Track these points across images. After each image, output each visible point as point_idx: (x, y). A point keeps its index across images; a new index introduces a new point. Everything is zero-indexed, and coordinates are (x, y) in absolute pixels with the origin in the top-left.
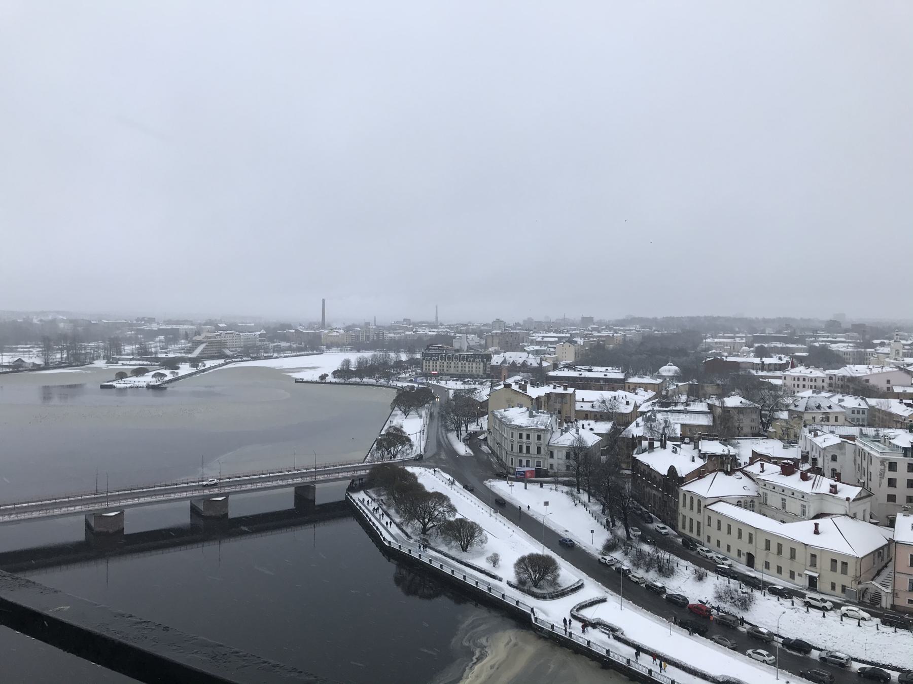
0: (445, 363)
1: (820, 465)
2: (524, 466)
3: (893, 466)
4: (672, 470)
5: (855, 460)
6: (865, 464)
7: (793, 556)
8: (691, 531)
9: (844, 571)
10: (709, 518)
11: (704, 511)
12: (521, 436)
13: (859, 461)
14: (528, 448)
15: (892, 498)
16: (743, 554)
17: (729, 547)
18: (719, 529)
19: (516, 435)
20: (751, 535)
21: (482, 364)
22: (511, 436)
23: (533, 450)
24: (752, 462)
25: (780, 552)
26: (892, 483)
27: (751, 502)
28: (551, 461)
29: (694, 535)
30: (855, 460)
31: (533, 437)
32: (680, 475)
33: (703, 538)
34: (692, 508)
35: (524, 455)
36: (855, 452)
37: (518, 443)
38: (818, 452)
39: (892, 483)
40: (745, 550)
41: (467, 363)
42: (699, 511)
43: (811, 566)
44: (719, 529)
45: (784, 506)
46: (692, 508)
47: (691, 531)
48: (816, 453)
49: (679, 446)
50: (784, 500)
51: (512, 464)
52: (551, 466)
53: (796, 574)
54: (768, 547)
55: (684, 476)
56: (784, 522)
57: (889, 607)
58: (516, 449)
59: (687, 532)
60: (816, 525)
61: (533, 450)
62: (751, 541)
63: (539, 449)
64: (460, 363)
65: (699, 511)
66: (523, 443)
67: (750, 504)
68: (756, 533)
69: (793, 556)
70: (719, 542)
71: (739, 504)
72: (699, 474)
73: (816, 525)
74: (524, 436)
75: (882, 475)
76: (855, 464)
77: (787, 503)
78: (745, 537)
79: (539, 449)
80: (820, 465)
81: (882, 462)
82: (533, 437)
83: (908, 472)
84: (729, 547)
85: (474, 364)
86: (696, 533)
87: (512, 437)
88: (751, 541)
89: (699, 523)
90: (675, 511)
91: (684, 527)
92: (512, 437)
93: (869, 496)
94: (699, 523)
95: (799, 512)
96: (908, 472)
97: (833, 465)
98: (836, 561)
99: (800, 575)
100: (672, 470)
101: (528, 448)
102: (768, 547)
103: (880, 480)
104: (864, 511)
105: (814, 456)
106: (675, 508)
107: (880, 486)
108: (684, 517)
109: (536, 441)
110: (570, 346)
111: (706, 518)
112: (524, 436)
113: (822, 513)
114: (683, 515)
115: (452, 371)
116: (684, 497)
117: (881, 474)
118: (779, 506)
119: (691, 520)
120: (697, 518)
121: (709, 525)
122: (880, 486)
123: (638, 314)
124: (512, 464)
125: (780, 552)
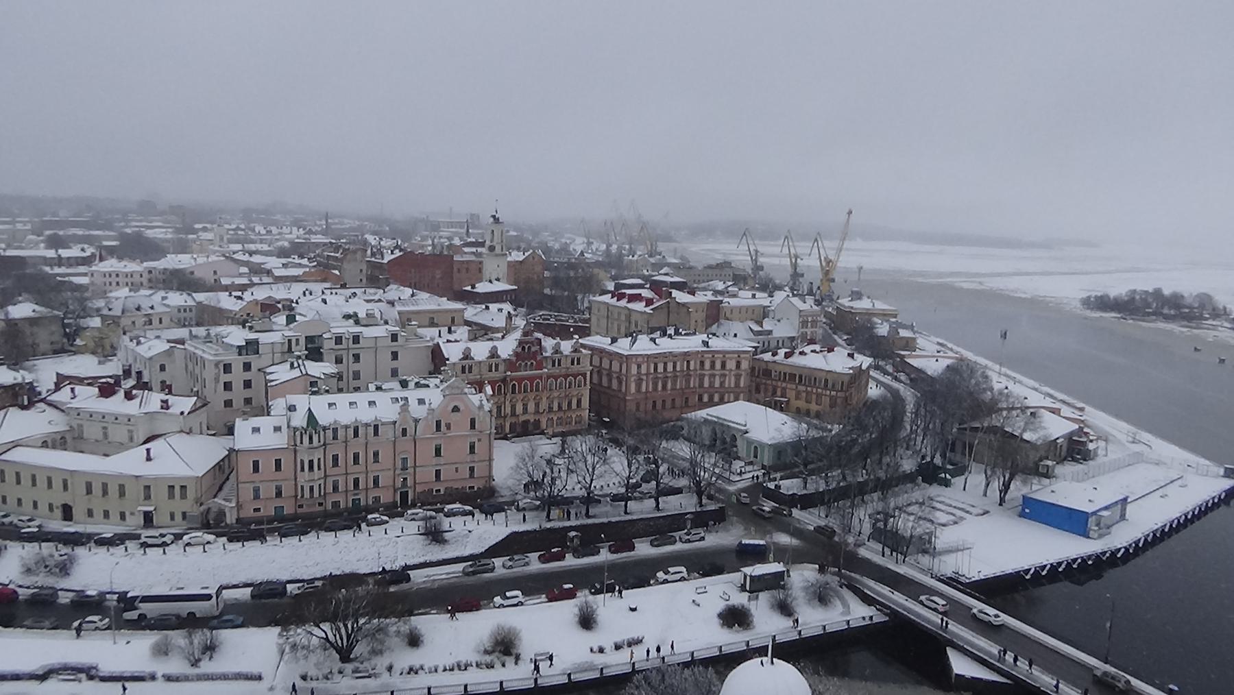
3: (227, 368)
5: (187, 366)
6: (197, 370)
7: (122, 493)
9: (183, 496)
13: (190, 367)
15: (228, 403)
16: (57, 508)
24: (58, 387)
25: (105, 493)
26: (228, 386)
30: (187, 366)
36: (186, 358)
38: (143, 363)
39: (228, 386)
43: (145, 499)
44: (18, 482)
45: (106, 435)
48: (141, 364)
53: (127, 514)
54: (89, 491)
57: (234, 521)
60: (148, 450)
62: (65, 487)
69: (122, 493)
70: (19, 500)
73: (148, 450)
75: (217, 380)
76: (187, 372)
78: (58, 484)
80: (146, 380)
81: (217, 365)
83: (244, 371)
84: (35, 505)
88: (65, 487)
93: (205, 405)
95: (125, 439)
96: (244, 371)
98: (173, 487)
99: (132, 514)
103: (216, 386)
104: (201, 423)
107: (216, 391)
116: (149, 442)
117: (215, 379)
118: (100, 436)
122: (216, 391)
125: (105, 493)
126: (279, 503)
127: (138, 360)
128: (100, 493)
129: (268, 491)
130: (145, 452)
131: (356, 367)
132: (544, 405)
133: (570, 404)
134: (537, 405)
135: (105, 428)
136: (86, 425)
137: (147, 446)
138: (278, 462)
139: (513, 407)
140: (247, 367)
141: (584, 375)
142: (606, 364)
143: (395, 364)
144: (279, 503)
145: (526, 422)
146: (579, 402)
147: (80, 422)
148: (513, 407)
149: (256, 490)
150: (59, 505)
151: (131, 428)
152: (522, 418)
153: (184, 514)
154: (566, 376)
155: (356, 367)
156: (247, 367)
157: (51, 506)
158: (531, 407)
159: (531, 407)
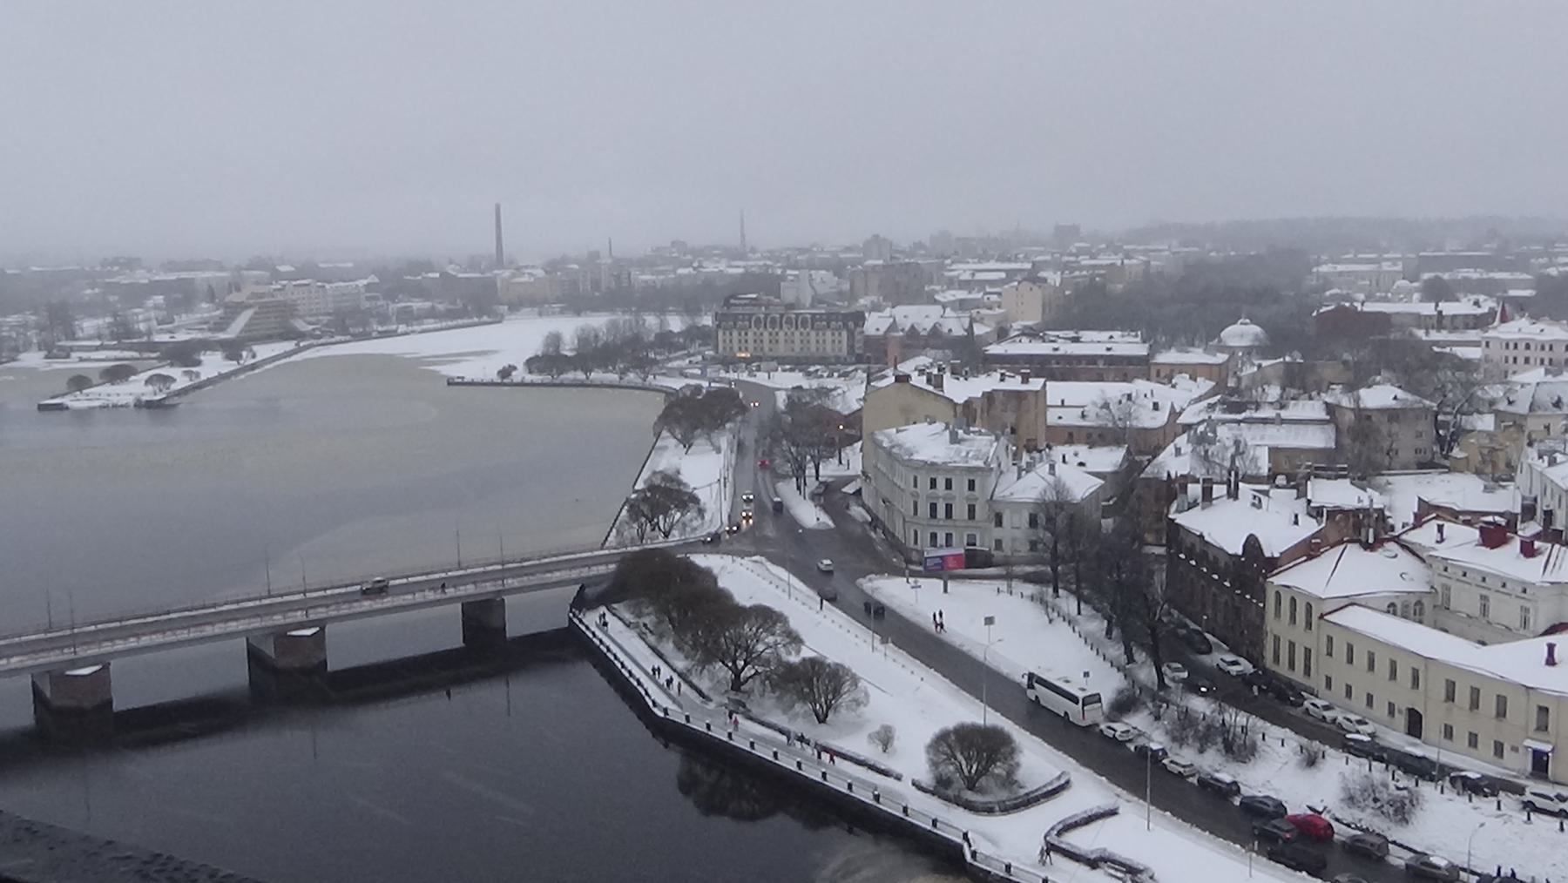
0: (766, 334)
1: (1559, 524)
2: (941, 546)
4: (1252, 544)
7: (1501, 713)
10: (1330, 639)
11: (1319, 626)
12: (933, 483)
14: (949, 508)
17: (1370, 698)
18: (1350, 660)
19: (924, 482)
21: (844, 334)
22: (912, 484)
23: (960, 511)
24: (1419, 522)
25: (1475, 704)
27: (1416, 604)
28: (997, 533)
29: (1298, 676)
31: (960, 485)
32: (1268, 554)
33: (1316, 681)
35: (941, 523)
37: (928, 497)
40: (1403, 704)
41: (813, 333)
42: (1309, 625)
43: (1538, 729)
44: (1350, 660)
45: (1484, 610)
47: (1292, 666)
48: (1552, 498)
49: (1266, 493)
50: (1484, 598)
51: (916, 542)
52: (999, 543)
53: (1507, 748)
54: (1450, 697)
55: (1277, 555)
56: (1484, 644)
58: (924, 509)
59: (1283, 669)
60: (1551, 647)
61: (960, 511)
63: (972, 510)
64: (797, 334)
65: (1309, 625)
66: (938, 498)
67: (1415, 611)
68: (1426, 667)
69: (1501, 713)
71: (1391, 609)
72: (1309, 550)
73: (1551, 647)
74: (941, 483)
77: (1492, 604)
78: (1404, 675)
79: (972, 510)
80: (1559, 524)
82: (960, 485)
84: (1370, 698)
85: (829, 333)
86: (1302, 672)
87: (916, 486)
89: (1308, 652)
90: (1258, 628)
91: (1277, 659)
92: (916, 486)
94: (1308, 652)
95: (1516, 623)
99: (1515, 749)
100: (1252, 544)
101: (949, 508)
102: (1450, 697)
105: (1548, 506)
106: (1258, 622)
108: (1277, 639)
109: (966, 492)
110: (1031, 289)
111: (1325, 640)
112: (941, 483)
113: (1562, 624)
114: (1275, 636)
115: (782, 350)
118: (1476, 612)
119: (1292, 645)
120: (1303, 639)
121: (1330, 654)
124: (916, 542)
125: (1475, 704)
127: (1549, 492)
128: (1467, 704)
130: (1546, 649)
135: (1484, 598)
136: (1454, 586)
147: (1444, 580)
150: (1404, 709)
151: (1528, 605)
157: (1391, 706)
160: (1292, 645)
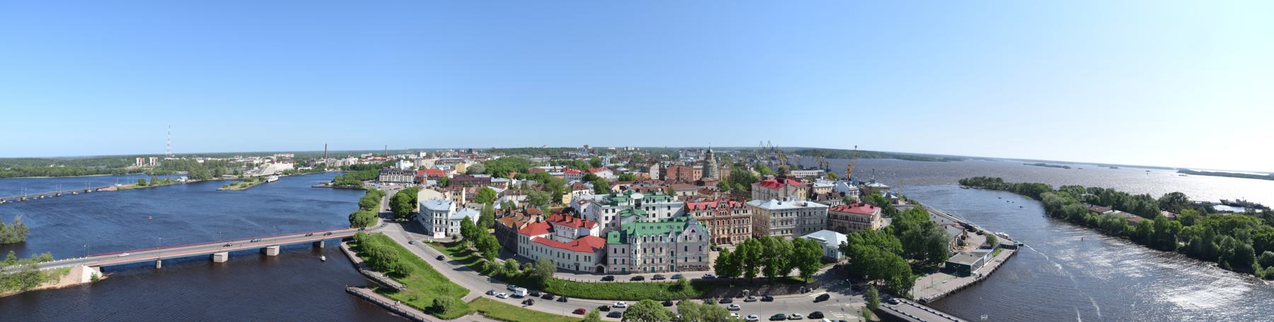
8: (524, 253)
20: (551, 251)
23: (444, 222)
25: (564, 257)
29: (525, 255)
34: (524, 243)
46: (524, 243)
47: (524, 253)
54: (558, 256)
59: (522, 254)
61: (444, 222)
62: (551, 254)
88: (551, 254)
90: (517, 245)
97: (585, 213)
102: (558, 256)
120: (529, 247)
123: (497, 146)
125: (564, 257)
126: (623, 266)
129: (619, 261)
131: (654, 212)
132: (732, 231)
133: (743, 232)
134: (729, 230)
137: (578, 240)
138: (623, 250)
139: (718, 231)
140: (614, 211)
141: (749, 217)
142: (759, 213)
143: (669, 211)
144: (623, 266)
145: (724, 239)
146: (747, 231)
148: (718, 231)
149: (615, 260)
152: (722, 237)
153: (590, 268)
154: (741, 218)
155: (654, 212)
156: (614, 211)
158: (726, 231)
159: (726, 231)
160: (524, 248)
